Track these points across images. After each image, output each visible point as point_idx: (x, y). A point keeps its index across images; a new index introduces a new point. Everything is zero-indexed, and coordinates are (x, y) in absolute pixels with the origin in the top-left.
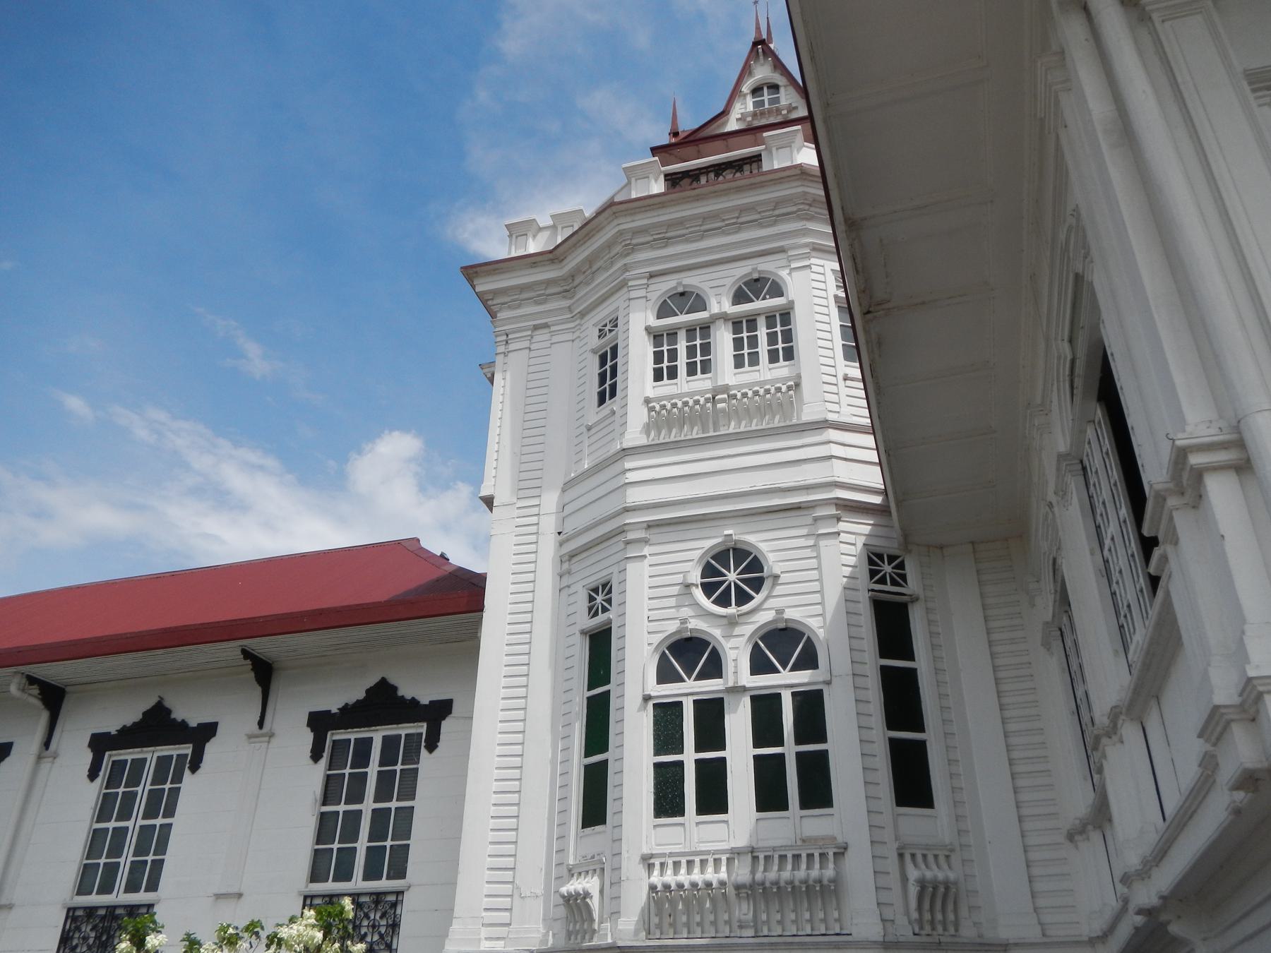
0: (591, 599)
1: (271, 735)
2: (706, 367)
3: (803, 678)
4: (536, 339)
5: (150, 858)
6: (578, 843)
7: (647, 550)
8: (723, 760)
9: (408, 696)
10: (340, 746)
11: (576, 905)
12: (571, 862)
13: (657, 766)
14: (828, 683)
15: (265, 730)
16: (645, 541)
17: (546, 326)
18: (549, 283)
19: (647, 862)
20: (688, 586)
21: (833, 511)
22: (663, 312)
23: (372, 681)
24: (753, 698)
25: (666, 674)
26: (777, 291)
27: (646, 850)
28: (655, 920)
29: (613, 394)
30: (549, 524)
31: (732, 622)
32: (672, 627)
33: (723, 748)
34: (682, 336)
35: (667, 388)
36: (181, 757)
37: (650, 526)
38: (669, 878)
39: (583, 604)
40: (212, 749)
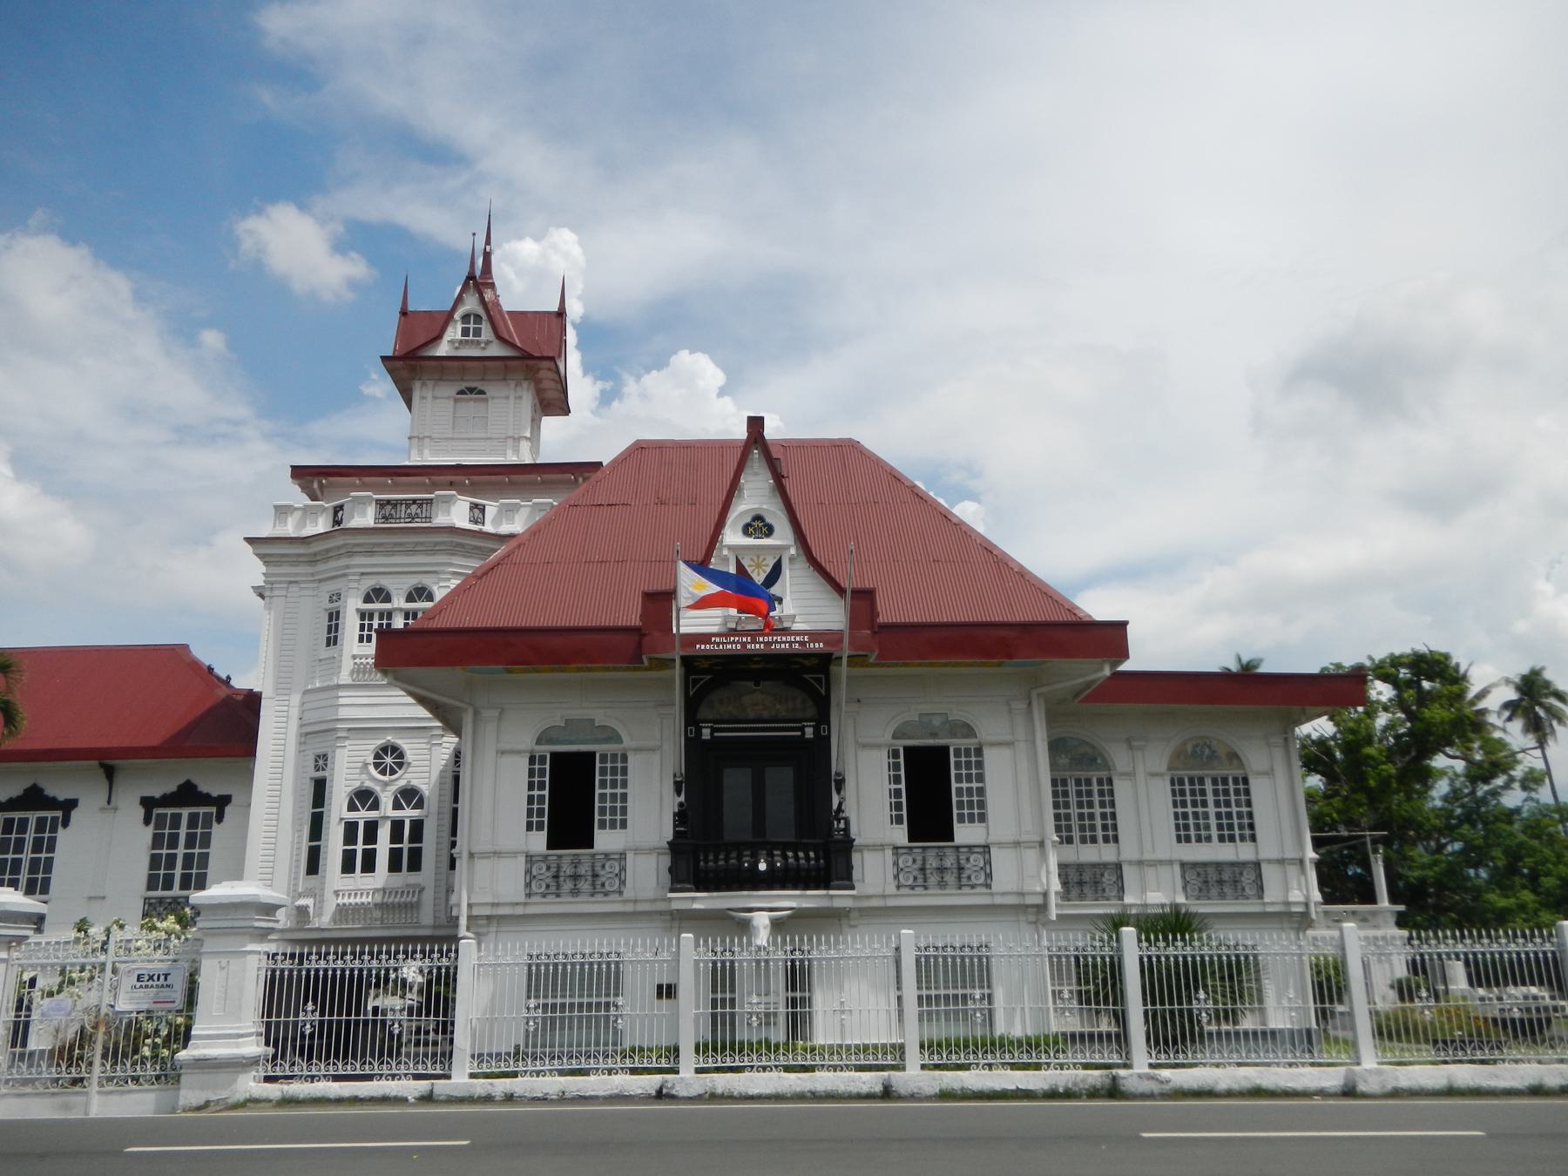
0: (316, 761)
1: (116, 809)
3: (416, 813)
4: (291, 589)
5: (40, 876)
6: (303, 881)
7: (347, 743)
8: (375, 850)
9: (205, 791)
10: (162, 817)
11: (302, 912)
12: (300, 890)
13: (344, 851)
14: (427, 816)
15: (112, 804)
16: (347, 738)
17: (296, 582)
18: (300, 555)
19: (337, 893)
20: (366, 764)
21: (441, 732)
22: (368, 599)
23: (181, 781)
24: (392, 822)
25: (352, 807)
27: (336, 889)
28: (338, 917)
29: (335, 644)
30: (295, 713)
31: (386, 784)
32: (357, 784)
33: (376, 843)
34: (376, 616)
36: (55, 819)
37: (350, 729)
38: (346, 901)
39: (311, 763)
40: (75, 815)
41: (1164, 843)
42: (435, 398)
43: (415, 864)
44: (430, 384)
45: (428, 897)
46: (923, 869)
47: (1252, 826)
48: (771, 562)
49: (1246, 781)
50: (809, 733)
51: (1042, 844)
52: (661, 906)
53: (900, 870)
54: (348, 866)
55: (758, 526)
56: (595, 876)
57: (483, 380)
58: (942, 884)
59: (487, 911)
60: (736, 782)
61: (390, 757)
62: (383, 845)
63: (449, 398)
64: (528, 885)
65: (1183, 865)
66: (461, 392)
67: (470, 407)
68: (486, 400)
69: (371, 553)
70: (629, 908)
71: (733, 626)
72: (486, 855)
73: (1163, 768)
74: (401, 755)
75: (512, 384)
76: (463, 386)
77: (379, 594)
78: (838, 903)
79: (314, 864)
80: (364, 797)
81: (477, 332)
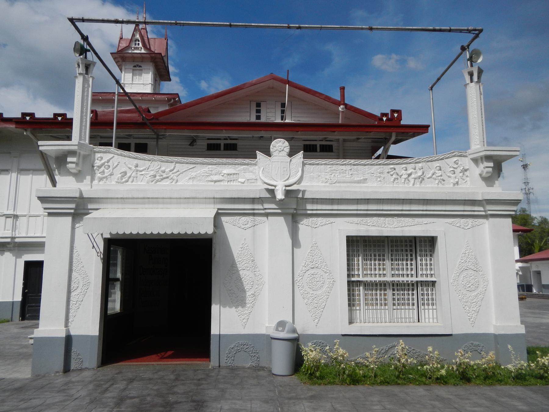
42: (125, 69)
57: (142, 62)
63: (130, 69)
68: (142, 70)
76: (136, 64)
81: (139, 44)
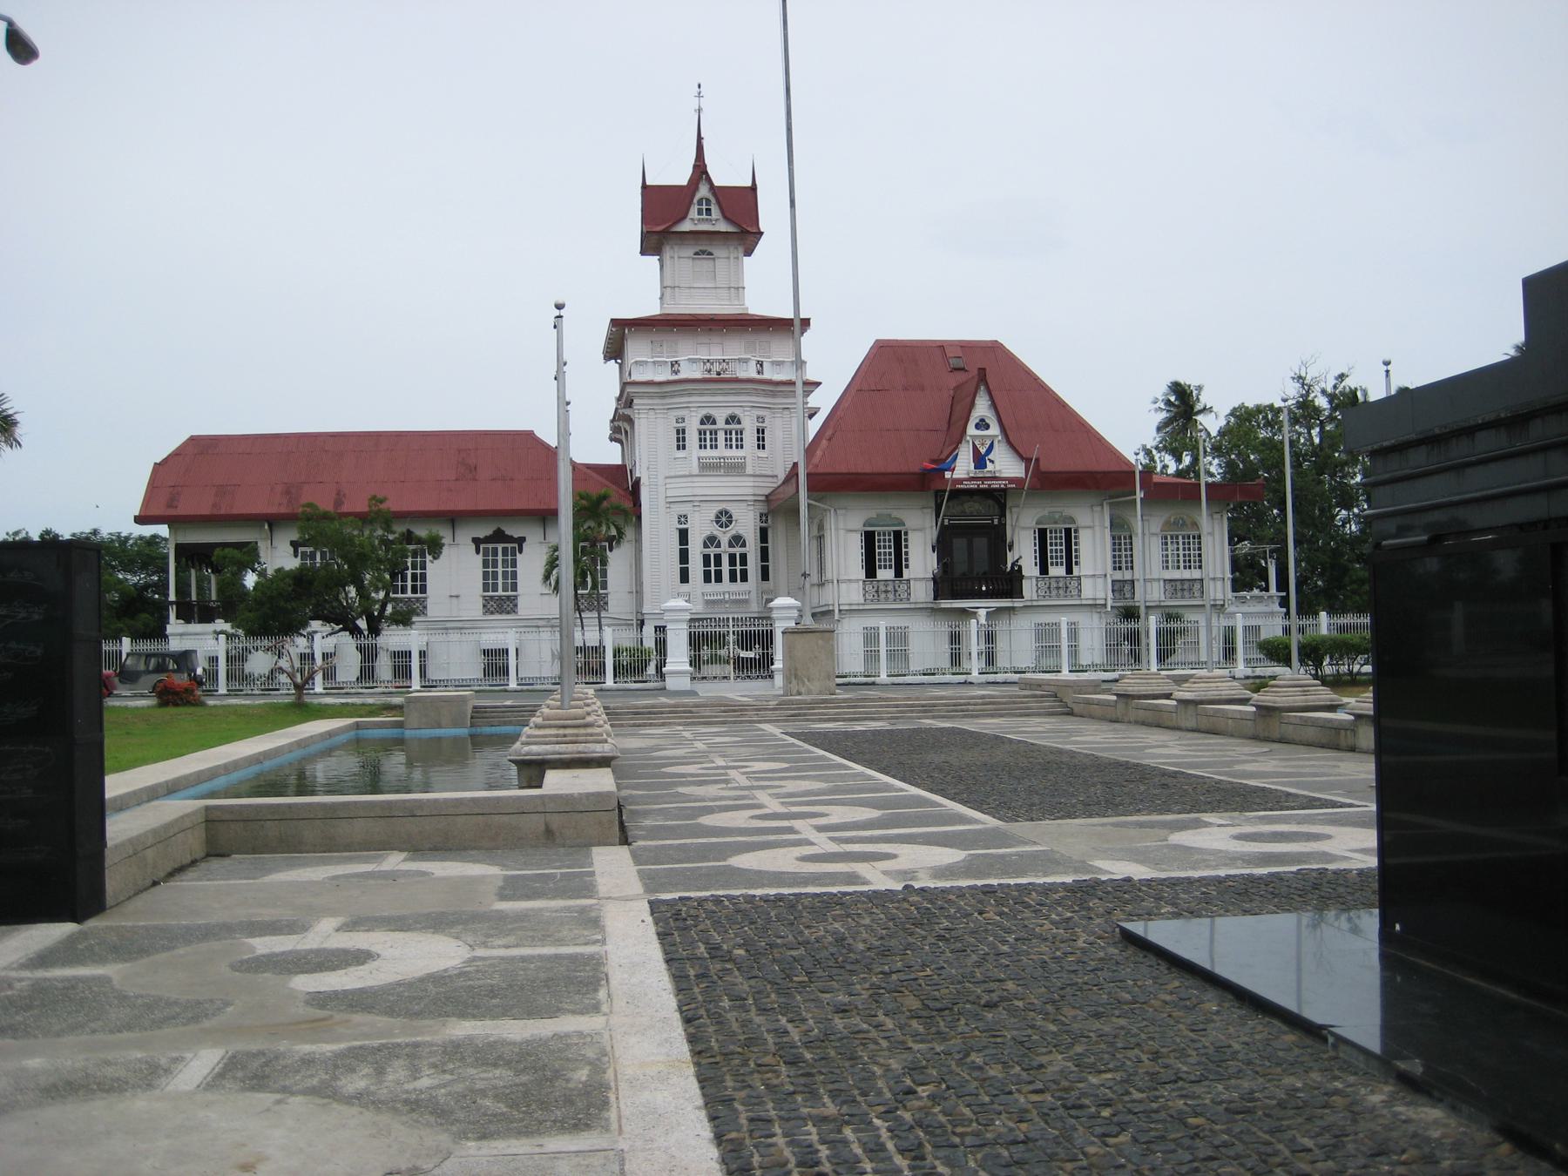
2: (716, 447)
25: (706, 546)
26: (739, 422)
34: (708, 433)
35: (703, 453)
40: (525, 546)
41: (1157, 571)
42: (679, 257)
43: (744, 578)
44: (676, 248)
45: (753, 595)
46: (1049, 588)
47: (1200, 561)
48: (989, 443)
49: (1199, 537)
50: (996, 521)
51: (1106, 575)
52: (930, 605)
53: (1038, 588)
54: (707, 579)
55: (982, 425)
56: (896, 591)
58: (1058, 596)
59: (847, 607)
60: (959, 544)
61: (724, 519)
62: (726, 568)
63: (689, 258)
64: (864, 595)
65: (1165, 580)
66: (696, 254)
67: (704, 265)
68: (714, 259)
69: (701, 394)
70: (913, 606)
71: (972, 475)
72: (845, 581)
73: (1159, 530)
74: (731, 516)
75: (732, 249)
76: (697, 249)
77: (708, 419)
78: (1016, 605)
79: (684, 577)
80: (711, 541)
81: (709, 211)
